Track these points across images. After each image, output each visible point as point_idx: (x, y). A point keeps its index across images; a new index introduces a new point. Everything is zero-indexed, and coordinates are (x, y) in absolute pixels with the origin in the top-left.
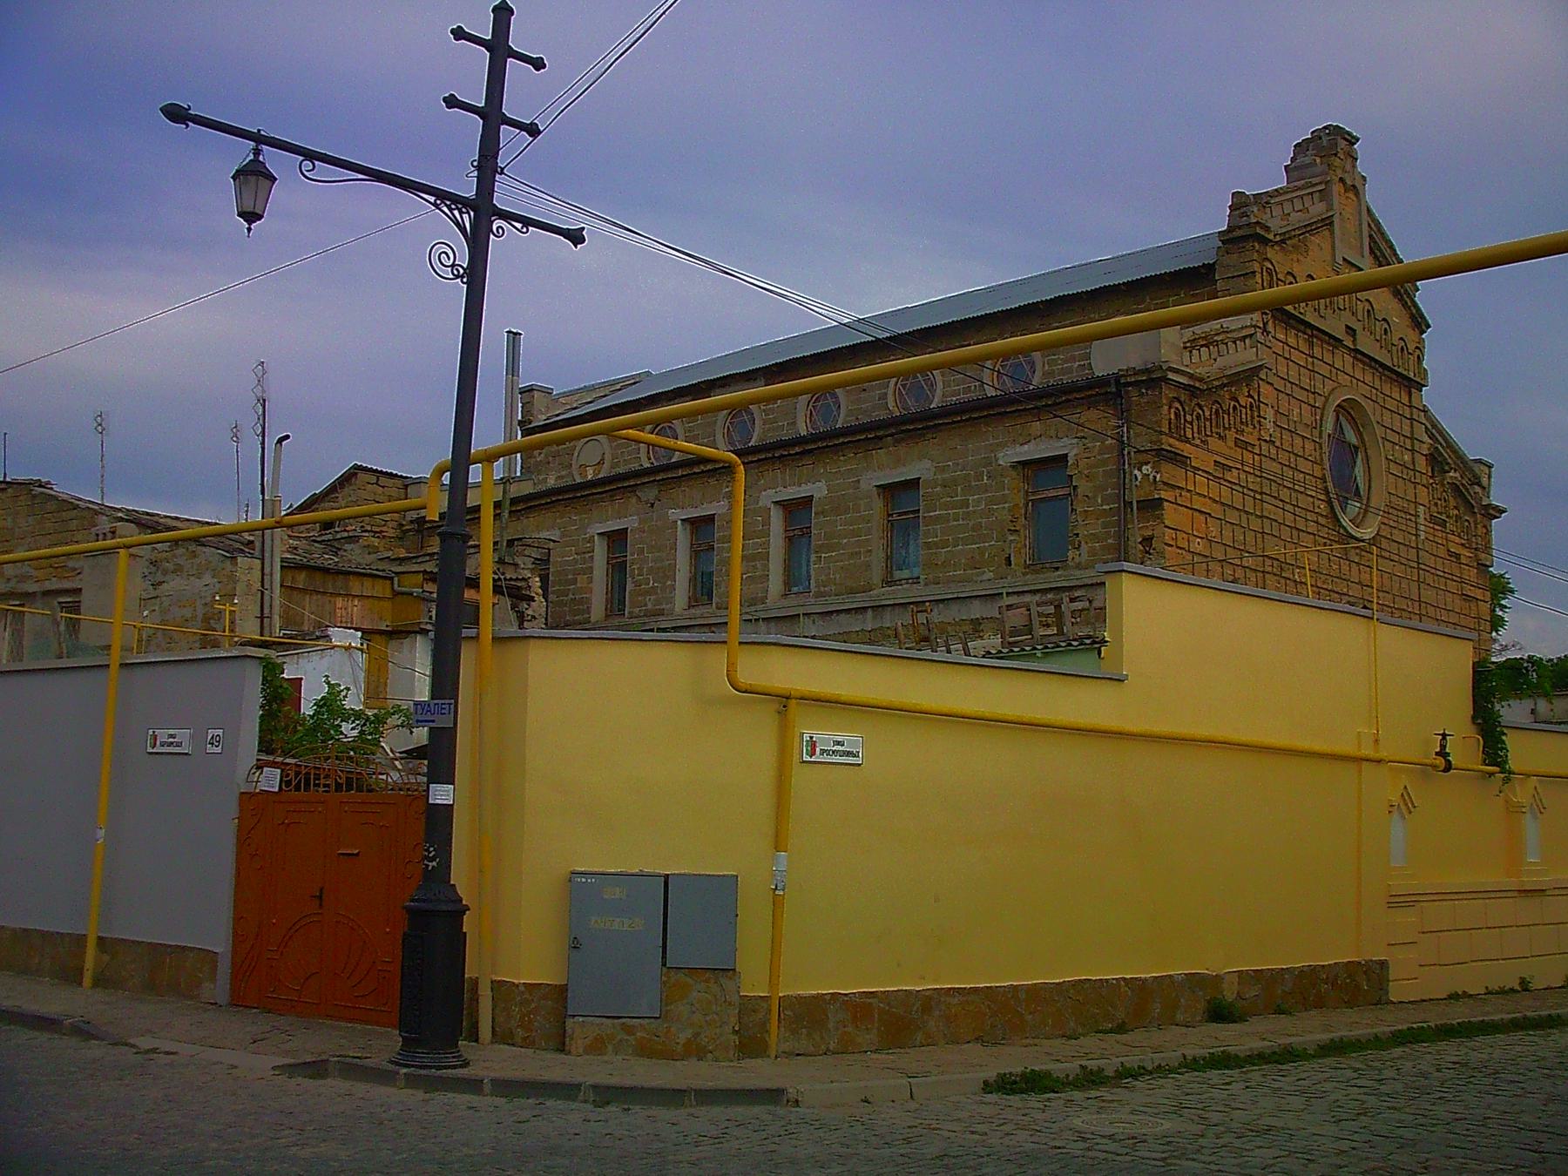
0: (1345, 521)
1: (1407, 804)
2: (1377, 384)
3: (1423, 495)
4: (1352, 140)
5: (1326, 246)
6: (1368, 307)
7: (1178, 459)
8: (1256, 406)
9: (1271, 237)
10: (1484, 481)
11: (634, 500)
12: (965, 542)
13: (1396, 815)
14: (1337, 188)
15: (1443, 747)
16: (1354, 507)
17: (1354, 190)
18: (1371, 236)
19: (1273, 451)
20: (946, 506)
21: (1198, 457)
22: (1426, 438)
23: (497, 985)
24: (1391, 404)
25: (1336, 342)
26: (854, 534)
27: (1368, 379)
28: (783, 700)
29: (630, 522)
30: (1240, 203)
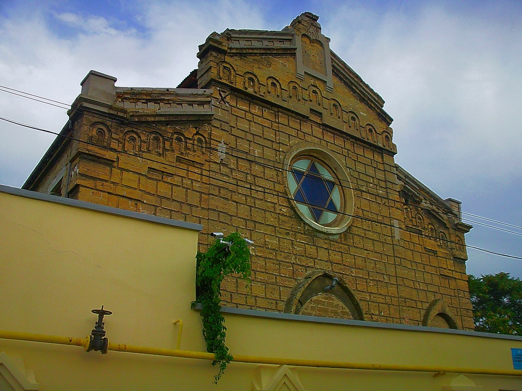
4: (315, 18)
6: (333, 102)
10: (455, 211)
21: (124, 161)
22: (398, 182)
25: (304, 118)
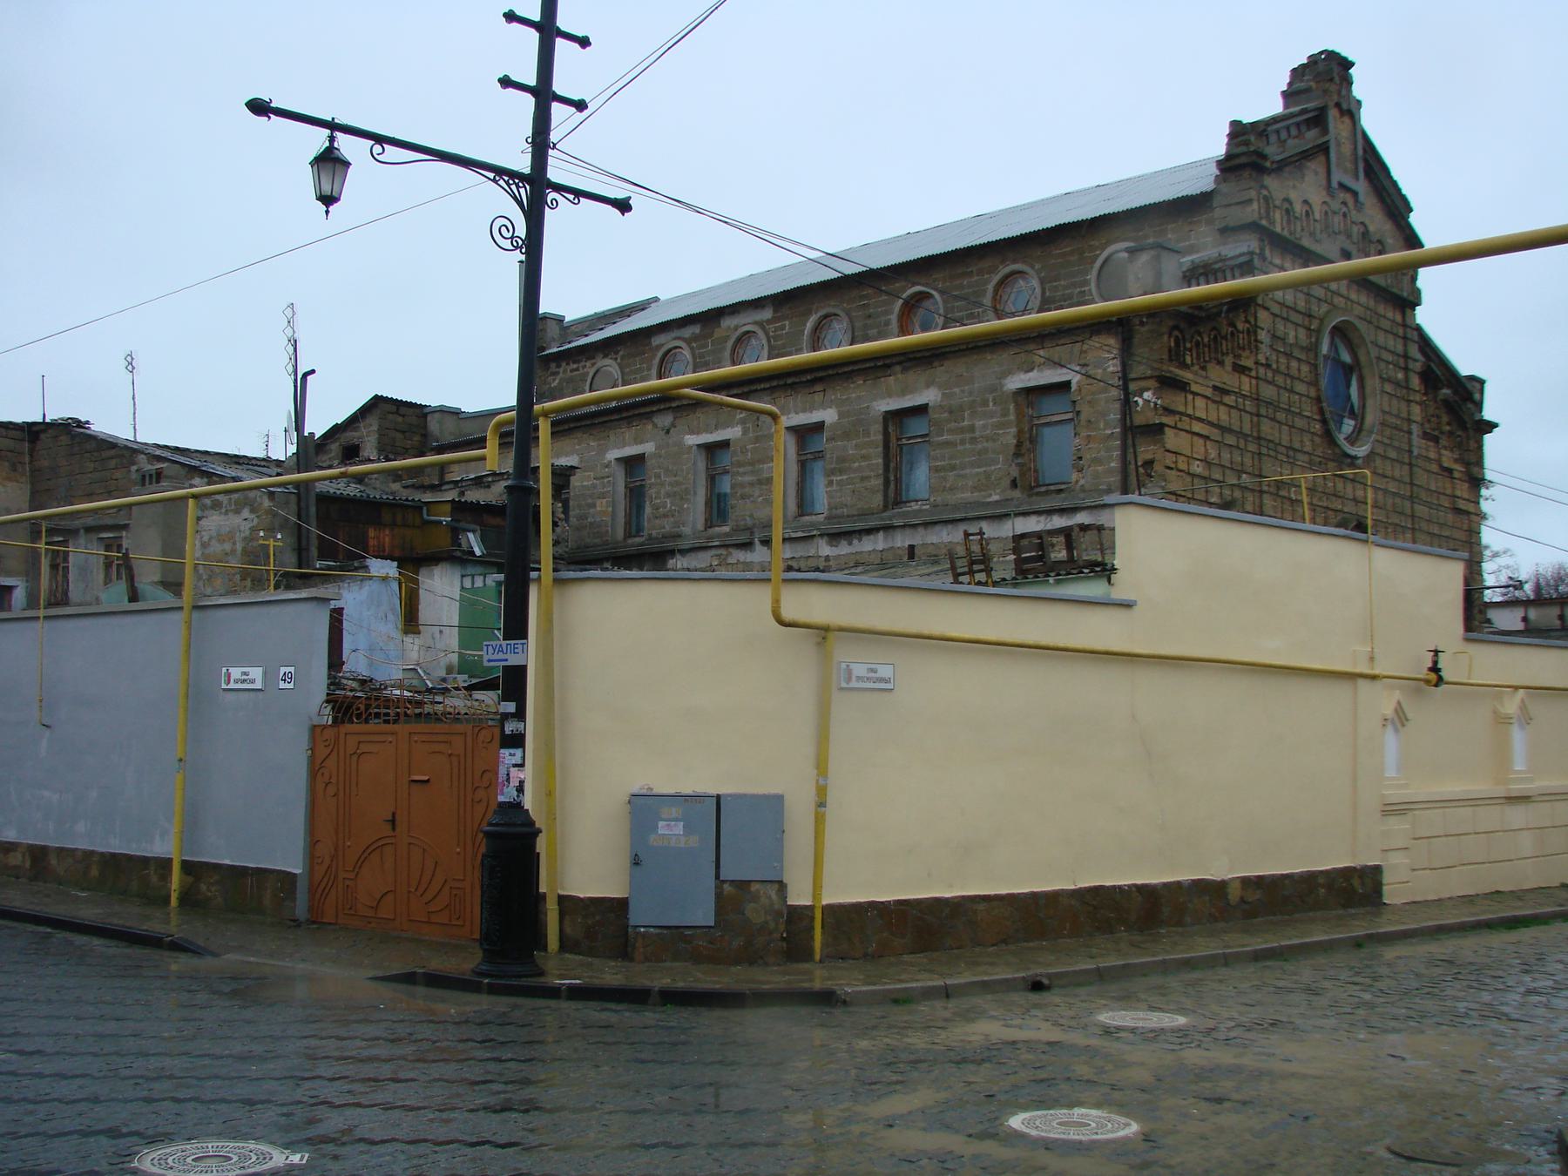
0: (1341, 438)
1: (1400, 718)
2: (1372, 303)
3: (1416, 409)
4: (1347, 65)
5: (1322, 171)
7: (1181, 386)
8: (1253, 331)
9: (1268, 164)
10: (1477, 396)
11: (650, 427)
12: (973, 465)
13: (1390, 729)
14: (1333, 114)
15: (1435, 663)
16: (1349, 425)
17: (1351, 111)
18: (1366, 161)
19: (1270, 374)
20: (951, 431)
22: (1419, 356)
23: (562, 899)
24: (1385, 324)
26: (864, 457)
27: (1363, 299)
28: (823, 632)
29: (648, 448)
30: (1238, 131)
